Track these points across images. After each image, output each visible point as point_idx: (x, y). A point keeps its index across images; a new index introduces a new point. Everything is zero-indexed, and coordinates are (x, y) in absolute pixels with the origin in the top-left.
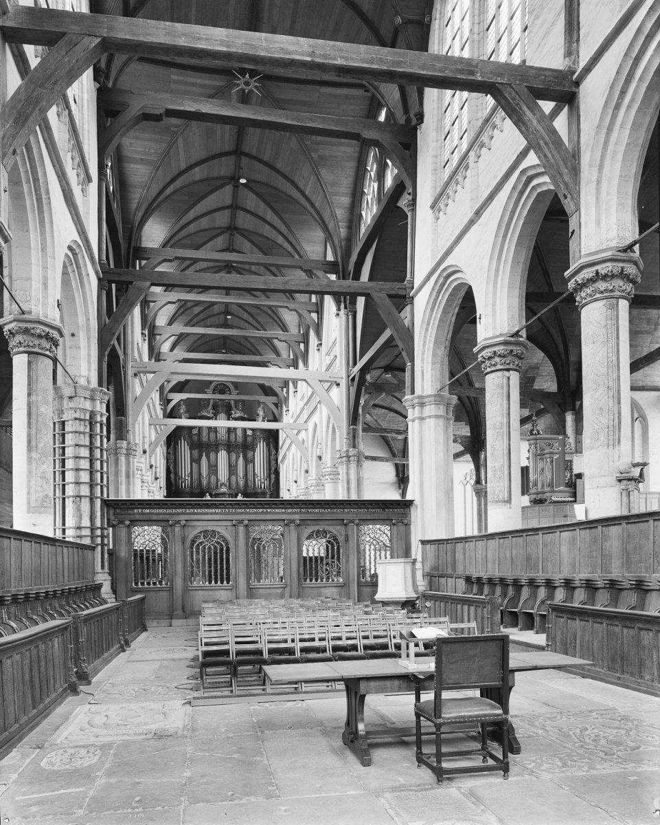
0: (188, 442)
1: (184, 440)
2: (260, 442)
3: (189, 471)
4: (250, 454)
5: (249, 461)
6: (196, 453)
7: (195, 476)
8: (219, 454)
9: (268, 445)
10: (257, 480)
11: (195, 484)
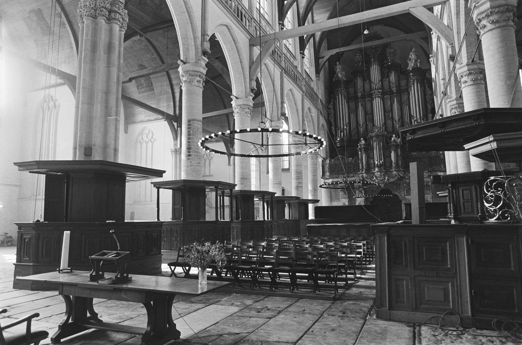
0: (344, 96)
1: (341, 95)
2: (414, 84)
3: (347, 121)
4: (405, 98)
5: (404, 104)
6: (352, 105)
7: (353, 125)
8: (374, 102)
9: (423, 85)
10: (413, 121)
11: (354, 132)
